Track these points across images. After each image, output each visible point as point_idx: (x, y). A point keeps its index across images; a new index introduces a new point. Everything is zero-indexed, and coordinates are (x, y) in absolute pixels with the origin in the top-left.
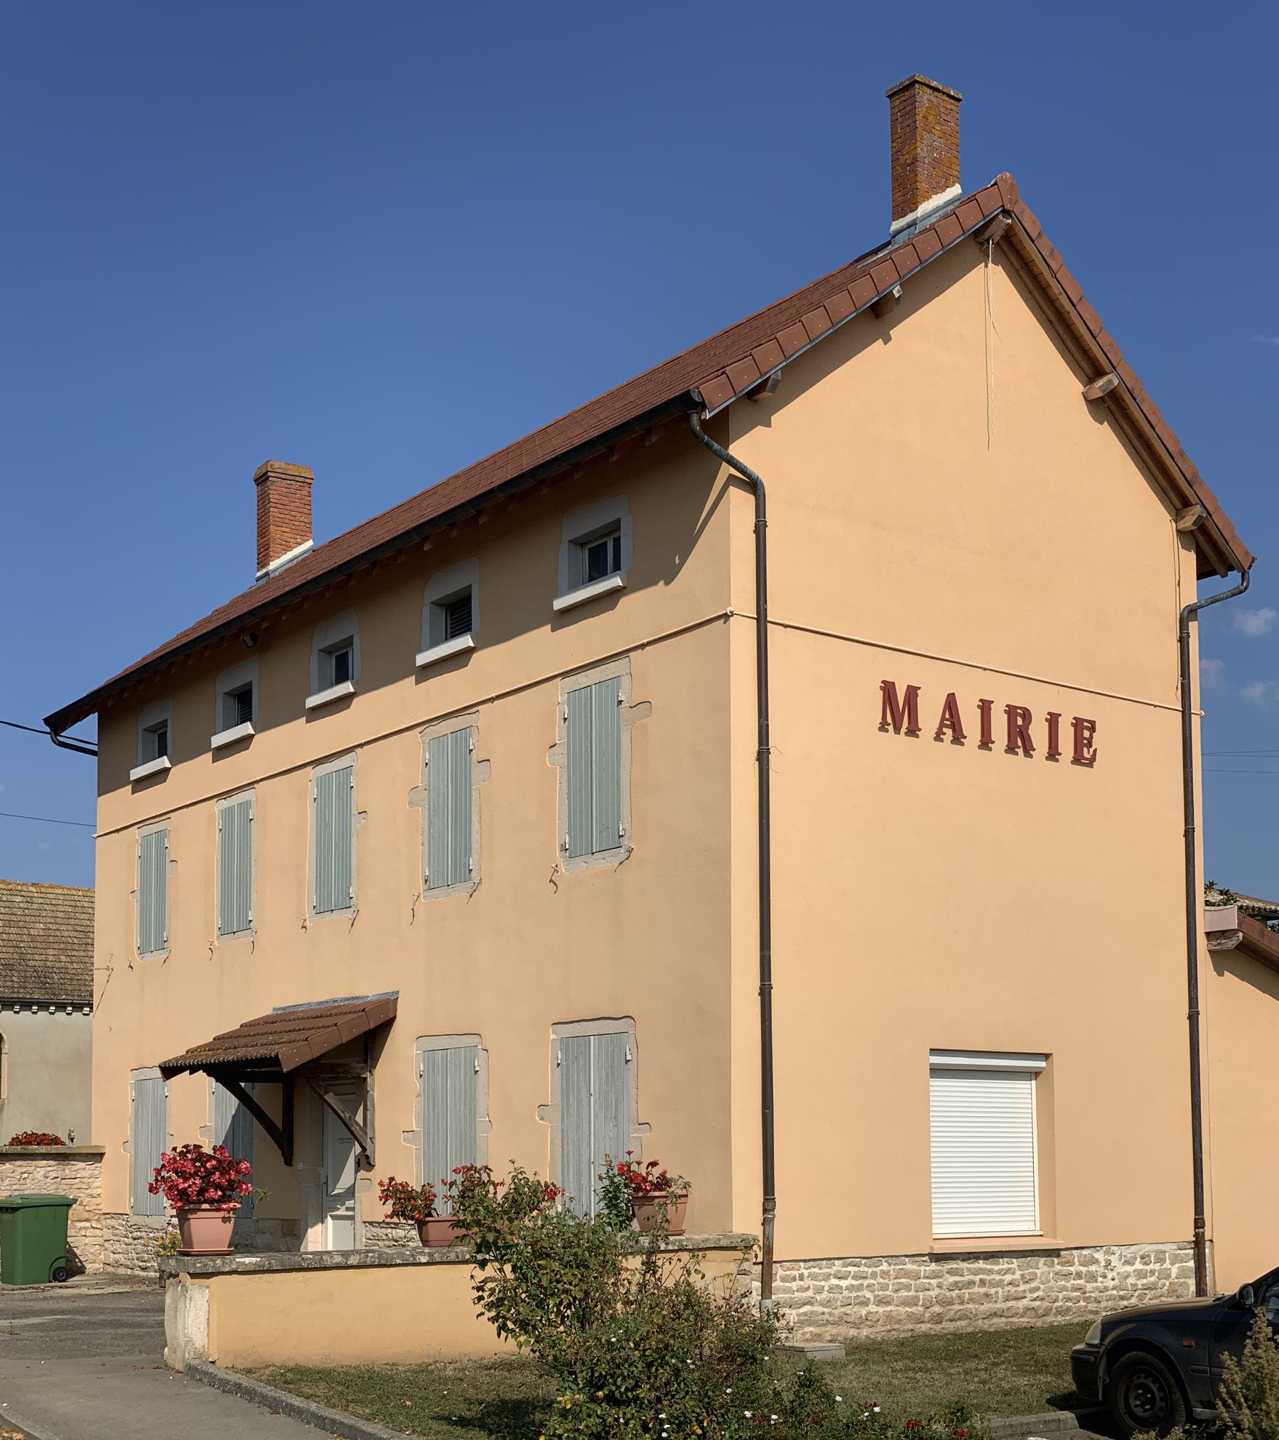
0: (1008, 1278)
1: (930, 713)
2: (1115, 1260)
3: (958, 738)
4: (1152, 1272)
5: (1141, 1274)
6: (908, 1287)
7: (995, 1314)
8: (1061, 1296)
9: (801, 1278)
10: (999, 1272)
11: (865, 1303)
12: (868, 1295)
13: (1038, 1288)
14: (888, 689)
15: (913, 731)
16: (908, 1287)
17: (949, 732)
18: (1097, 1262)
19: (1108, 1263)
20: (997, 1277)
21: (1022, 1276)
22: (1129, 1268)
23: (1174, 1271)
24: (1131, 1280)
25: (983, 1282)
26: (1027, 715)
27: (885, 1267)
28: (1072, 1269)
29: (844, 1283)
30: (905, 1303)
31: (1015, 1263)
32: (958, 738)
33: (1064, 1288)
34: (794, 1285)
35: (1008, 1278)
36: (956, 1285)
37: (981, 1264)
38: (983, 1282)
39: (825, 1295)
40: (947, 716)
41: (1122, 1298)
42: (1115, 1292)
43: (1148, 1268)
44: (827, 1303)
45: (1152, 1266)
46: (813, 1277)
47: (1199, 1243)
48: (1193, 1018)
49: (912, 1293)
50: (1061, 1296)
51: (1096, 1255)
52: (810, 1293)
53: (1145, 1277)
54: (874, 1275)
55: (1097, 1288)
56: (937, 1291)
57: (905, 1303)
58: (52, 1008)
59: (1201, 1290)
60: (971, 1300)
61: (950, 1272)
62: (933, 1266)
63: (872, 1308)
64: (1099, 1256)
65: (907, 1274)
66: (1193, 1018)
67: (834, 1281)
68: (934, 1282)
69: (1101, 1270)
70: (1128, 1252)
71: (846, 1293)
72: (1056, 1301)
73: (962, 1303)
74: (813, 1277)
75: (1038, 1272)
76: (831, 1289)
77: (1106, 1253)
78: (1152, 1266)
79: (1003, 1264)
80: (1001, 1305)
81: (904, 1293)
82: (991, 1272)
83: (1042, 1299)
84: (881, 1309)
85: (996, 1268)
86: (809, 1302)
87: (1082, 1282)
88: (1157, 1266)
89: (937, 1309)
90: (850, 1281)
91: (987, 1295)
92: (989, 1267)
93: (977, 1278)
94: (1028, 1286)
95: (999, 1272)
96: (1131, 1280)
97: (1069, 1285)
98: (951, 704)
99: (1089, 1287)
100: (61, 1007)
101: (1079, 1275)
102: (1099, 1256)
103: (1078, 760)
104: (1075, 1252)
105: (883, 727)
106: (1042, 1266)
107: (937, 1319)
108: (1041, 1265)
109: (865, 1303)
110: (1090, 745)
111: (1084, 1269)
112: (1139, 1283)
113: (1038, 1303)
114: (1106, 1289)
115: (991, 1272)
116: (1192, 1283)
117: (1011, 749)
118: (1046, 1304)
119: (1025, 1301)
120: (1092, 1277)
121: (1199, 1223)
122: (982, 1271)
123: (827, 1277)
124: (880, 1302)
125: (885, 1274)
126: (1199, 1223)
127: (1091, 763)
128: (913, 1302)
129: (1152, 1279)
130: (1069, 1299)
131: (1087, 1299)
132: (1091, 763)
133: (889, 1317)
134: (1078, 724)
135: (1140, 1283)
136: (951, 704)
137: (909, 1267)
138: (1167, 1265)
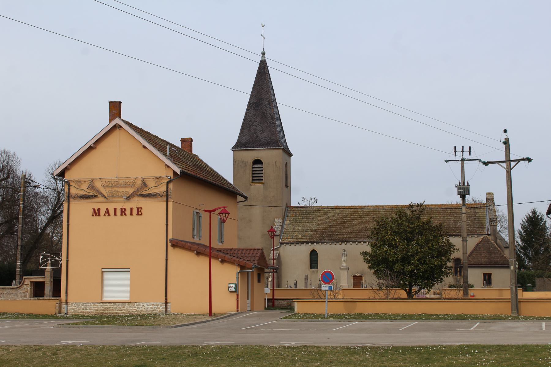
0: (118, 307)
1: (102, 212)
4: (155, 308)
5: (151, 308)
6: (96, 308)
7: (115, 313)
8: (131, 311)
9: (74, 305)
10: (116, 306)
11: (87, 309)
12: (87, 308)
13: (125, 309)
14: (94, 210)
15: (99, 215)
16: (96, 308)
17: (107, 214)
18: (141, 305)
19: (143, 306)
20: (116, 307)
21: (122, 307)
22: (149, 307)
23: (161, 308)
24: (148, 309)
25: (112, 308)
26: (125, 209)
27: (91, 304)
28: (134, 306)
29: (83, 306)
30: (95, 310)
32: (109, 215)
33: (131, 309)
34: (73, 306)
35: (118, 307)
36: (106, 308)
37: (112, 304)
38: (112, 308)
39: (79, 308)
40: (107, 212)
41: (147, 312)
42: (144, 311)
43: (154, 307)
44: (79, 309)
45: (155, 307)
46: (77, 305)
47: (166, 303)
48: (167, 260)
49: (97, 308)
50: (131, 311)
51: (140, 304)
52: (76, 307)
53: (153, 308)
54: (89, 305)
55: (140, 310)
56: (102, 308)
57: (95, 310)
58: (335, 243)
59: (166, 311)
60: (109, 310)
61: (105, 305)
62: (102, 304)
63: (88, 310)
64: (141, 304)
65: (96, 305)
66: (167, 260)
67: (81, 306)
68: (102, 307)
69: (141, 307)
70: (148, 304)
71: (83, 308)
72: (129, 311)
73: (108, 311)
74: (77, 305)
75: (125, 306)
76: (80, 307)
77: (143, 304)
78: (155, 307)
79: (117, 304)
80: (116, 312)
81: (95, 308)
82: (114, 306)
83: (126, 311)
84: (90, 311)
85: (115, 305)
86: (75, 309)
87: (136, 309)
88: (156, 307)
89: (102, 311)
90: (84, 306)
91: (113, 310)
92: (114, 305)
93: (111, 307)
94: (123, 309)
95: (116, 306)
96: (148, 309)
97: (133, 309)
98: (107, 209)
99: (138, 309)
102: (141, 304)
103: (138, 214)
104: (135, 303)
105: (93, 215)
106: (127, 305)
107: (102, 313)
108: (127, 305)
110: (140, 211)
111: (137, 306)
112: (151, 309)
113: (125, 312)
114: (142, 310)
115: (114, 306)
116: (165, 310)
117: (121, 215)
118: (127, 312)
119: (122, 311)
120: (139, 308)
121: (166, 299)
122: (112, 306)
123: (80, 305)
124: (90, 310)
125: (91, 305)
126: (166, 299)
127: (141, 214)
129: (155, 309)
130: (132, 311)
131: (138, 312)
132: (141, 214)
133: (91, 312)
134: (138, 209)
135: (151, 309)
136: (107, 209)
137: (96, 304)
138: (159, 306)
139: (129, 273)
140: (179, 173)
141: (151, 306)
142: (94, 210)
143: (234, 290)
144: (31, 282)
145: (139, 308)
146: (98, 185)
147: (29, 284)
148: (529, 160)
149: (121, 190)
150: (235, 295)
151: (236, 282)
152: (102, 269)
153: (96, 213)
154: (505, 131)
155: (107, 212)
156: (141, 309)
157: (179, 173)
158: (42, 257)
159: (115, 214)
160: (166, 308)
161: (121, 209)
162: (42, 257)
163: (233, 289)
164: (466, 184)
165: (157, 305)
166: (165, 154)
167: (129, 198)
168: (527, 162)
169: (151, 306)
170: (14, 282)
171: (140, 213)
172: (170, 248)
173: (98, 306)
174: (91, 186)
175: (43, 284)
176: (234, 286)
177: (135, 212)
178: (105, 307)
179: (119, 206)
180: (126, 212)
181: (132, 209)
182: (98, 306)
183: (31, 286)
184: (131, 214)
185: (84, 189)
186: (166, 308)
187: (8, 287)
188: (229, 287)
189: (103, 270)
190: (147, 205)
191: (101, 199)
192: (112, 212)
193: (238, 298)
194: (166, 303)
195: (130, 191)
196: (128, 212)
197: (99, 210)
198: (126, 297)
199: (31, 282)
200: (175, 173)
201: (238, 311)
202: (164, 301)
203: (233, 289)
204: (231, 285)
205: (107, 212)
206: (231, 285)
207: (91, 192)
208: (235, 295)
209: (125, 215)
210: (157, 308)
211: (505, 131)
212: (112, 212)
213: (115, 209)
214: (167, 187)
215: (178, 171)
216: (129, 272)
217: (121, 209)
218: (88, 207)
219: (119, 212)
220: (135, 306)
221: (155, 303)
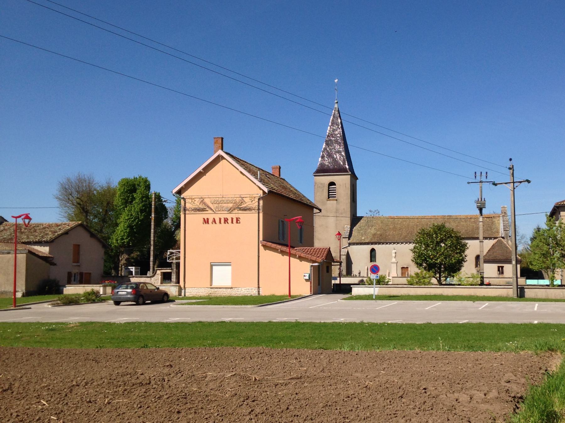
1: (210, 221)
2: (242, 289)
3: (215, 223)
5: (247, 291)
14: (204, 219)
15: (208, 223)
23: (255, 291)
24: (246, 292)
26: (227, 219)
31: (224, 289)
37: (218, 289)
47: (259, 287)
48: (259, 257)
63: (201, 294)
66: (259, 257)
70: (245, 288)
79: (222, 289)
100: (387, 243)
101: (235, 291)
102: (240, 289)
103: (237, 222)
106: (229, 290)
109: (199, 293)
117: (225, 223)
120: (238, 291)
121: (259, 285)
126: (259, 285)
127: (240, 223)
128: (207, 293)
132: (240, 223)
134: (237, 218)
138: (253, 290)
139: (230, 267)
140: (267, 192)
141: (247, 290)
142: (204, 219)
143: (308, 278)
144: (161, 272)
145: (238, 291)
146: (207, 201)
147: (160, 275)
148: (528, 181)
149: (224, 205)
150: (309, 283)
151: (309, 272)
152: (211, 263)
153: (206, 221)
154: (511, 160)
155: (214, 221)
156: (240, 292)
157: (267, 192)
158: (168, 253)
159: (220, 222)
160: (259, 292)
161: (225, 219)
162: (168, 253)
163: (307, 278)
164: (483, 200)
165: (252, 289)
166: (256, 178)
167: (230, 210)
168: (526, 183)
169: (247, 290)
170: (149, 272)
171: (238, 222)
172: (261, 248)
173: (208, 290)
174: (202, 202)
175: (170, 273)
176: (308, 275)
177: (235, 221)
178: (213, 291)
179: (223, 217)
180: (228, 221)
181: (232, 219)
182: (208, 290)
183: (161, 275)
184: (232, 222)
185: (197, 204)
186: (259, 292)
187: (144, 276)
188: (304, 276)
189: (212, 264)
190: (243, 216)
191: (210, 212)
192: (217, 221)
193: (311, 284)
194: (259, 287)
195: (231, 205)
196: (230, 221)
197: (208, 219)
198: (229, 284)
199: (161, 272)
200: (264, 192)
201: (311, 293)
202: (257, 286)
203: (307, 278)
204: (306, 275)
205: (214, 221)
206: (306, 275)
207: (201, 206)
208: (309, 283)
209: (227, 222)
210: (251, 292)
211: (511, 160)
212: (217, 221)
213: (220, 219)
214: (259, 203)
215: (266, 190)
216: (230, 265)
217: (225, 219)
218: (200, 217)
219: (223, 221)
220: (236, 290)
221: (250, 288)
